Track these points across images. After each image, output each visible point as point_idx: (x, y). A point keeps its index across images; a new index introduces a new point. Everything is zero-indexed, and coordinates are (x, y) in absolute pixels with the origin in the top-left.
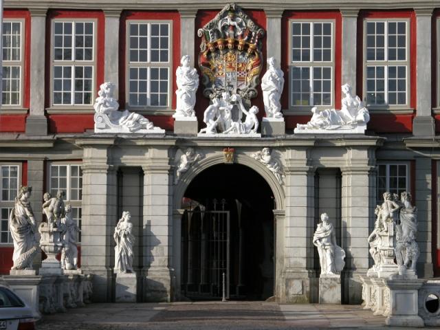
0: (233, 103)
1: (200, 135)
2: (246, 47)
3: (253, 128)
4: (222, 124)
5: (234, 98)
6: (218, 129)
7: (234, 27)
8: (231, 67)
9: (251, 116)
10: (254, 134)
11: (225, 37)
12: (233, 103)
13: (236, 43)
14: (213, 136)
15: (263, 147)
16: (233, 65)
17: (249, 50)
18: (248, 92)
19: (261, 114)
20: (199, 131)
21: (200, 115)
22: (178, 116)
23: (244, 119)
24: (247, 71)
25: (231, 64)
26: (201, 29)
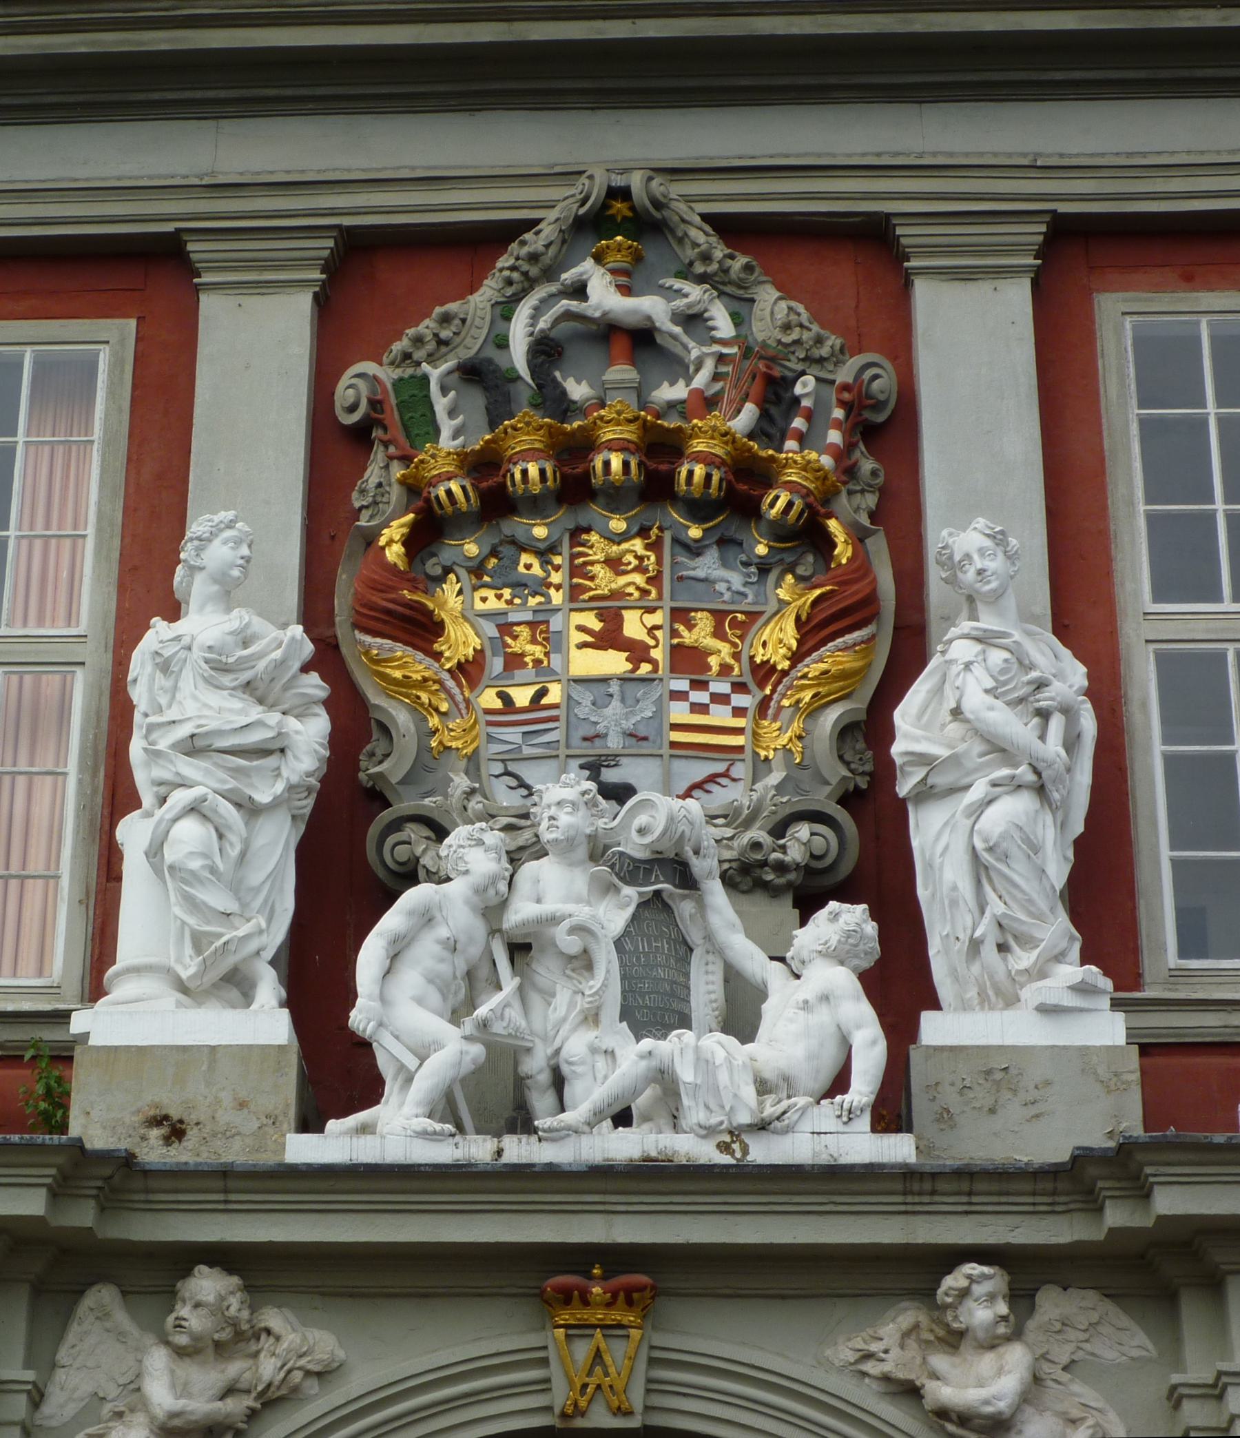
0: (632, 871)
1: (304, 1149)
2: (744, 484)
3: (840, 1083)
4: (536, 1065)
5: (658, 812)
6: (502, 1093)
7: (640, 340)
8: (610, 638)
9: (815, 987)
10: (844, 1137)
11: (562, 407)
12: (632, 871)
13: (660, 447)
14: (443, 1153)
15: (955, 1256)
16: (634, 626)
17: (777, 503)
18: (779, 830)
19: (899, 983)
20: (310, 1122)
21: (316, 974)
22: (129, 1019)
23: (741, 1017)
24: (764, 672)
25: (612, 619)
26: (369, 367)
